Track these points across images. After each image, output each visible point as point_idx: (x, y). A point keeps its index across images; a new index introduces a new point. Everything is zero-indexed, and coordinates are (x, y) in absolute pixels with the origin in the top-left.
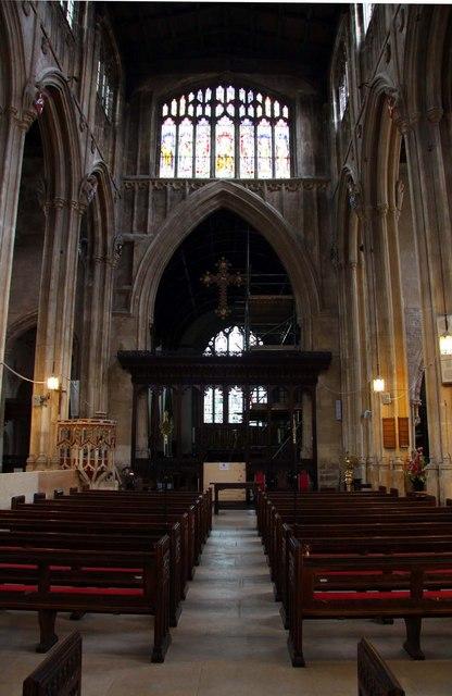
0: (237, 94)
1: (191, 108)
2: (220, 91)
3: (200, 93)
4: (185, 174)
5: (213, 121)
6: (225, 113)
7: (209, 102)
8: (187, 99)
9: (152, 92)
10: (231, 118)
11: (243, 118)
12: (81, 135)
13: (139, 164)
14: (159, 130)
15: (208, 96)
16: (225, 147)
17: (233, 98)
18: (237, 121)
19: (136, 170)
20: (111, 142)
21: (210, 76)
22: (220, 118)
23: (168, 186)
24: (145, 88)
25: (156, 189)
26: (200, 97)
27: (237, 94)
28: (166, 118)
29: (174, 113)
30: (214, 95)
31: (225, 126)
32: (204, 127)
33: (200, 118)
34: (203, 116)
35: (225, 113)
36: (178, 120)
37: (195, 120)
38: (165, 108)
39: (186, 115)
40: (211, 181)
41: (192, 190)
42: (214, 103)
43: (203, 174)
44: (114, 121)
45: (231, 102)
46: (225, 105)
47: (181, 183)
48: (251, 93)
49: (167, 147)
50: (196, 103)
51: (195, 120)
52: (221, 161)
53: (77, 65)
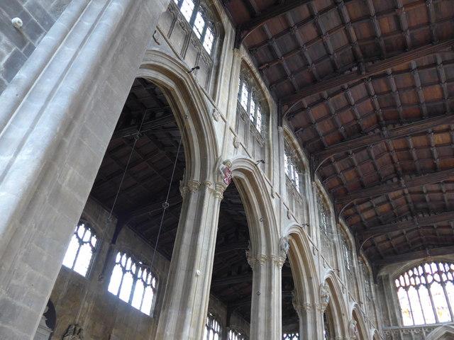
0: (438, 267)
1: (412, 279)
2: (427, 266)
3: (415, 269)
4: (419, 322)
5: (428, 286)
6: (434, 280)
7: (422, 275)
8: (408, 274)
9: (387, 276)
10: (439, 283)
11: (446, 282)
12: (366, 324)
13: (390, 319)
14: (397, 295)
15: (421, 272)
16: (440, 301)
17: (437, 270)
18: (443, 283)
19: (390, 323)
20: (373, 311)
21: (419, 260)
22: (431, 283)
23: (412, 332)
24: (383, 273)
25: (404, 335)
26: (416, 272)
27: (438, 267)
28: (399, 288)
29: (403, 284)
30: (424, 270)
31: (436, 288)
32: (423, 289)
33: (419, 285)
34: (421, 284)
35: (434, 280)
36: (406, 288)
37: (417, 287)
38: (397, 281)
39: (411, 285)
40: (438, 327)
41: (427, 333)
42: (425, 274)
43: (431, 321)
44: (372, 298)
45: (436, 272)
46: (432, 275)
47: (419, 329)
48: (446, 265)
49: (404, 305)
50: (414, 276)
51: (417, 287)
52: (440, 311)
53: (355, 286)
